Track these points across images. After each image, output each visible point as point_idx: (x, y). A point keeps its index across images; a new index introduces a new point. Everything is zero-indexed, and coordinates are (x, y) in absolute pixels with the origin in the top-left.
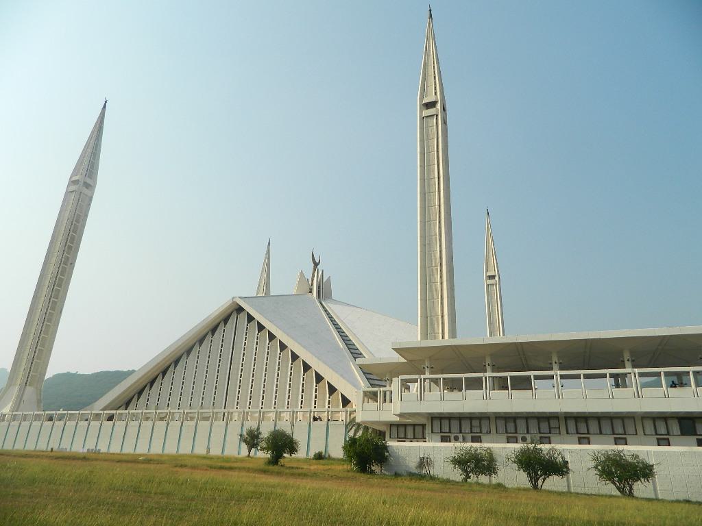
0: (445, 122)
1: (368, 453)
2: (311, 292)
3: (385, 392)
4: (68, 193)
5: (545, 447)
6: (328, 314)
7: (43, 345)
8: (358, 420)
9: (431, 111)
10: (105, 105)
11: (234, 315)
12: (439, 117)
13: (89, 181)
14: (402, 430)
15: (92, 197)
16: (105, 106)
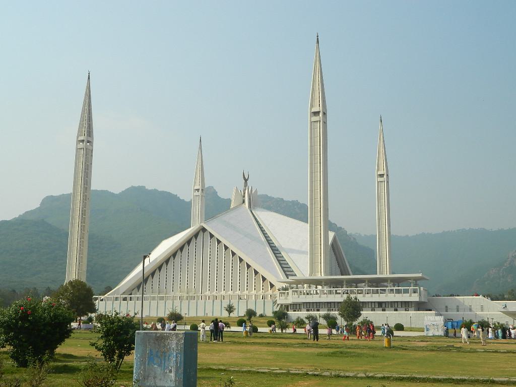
0: (325, 123)
1: (281, 317)
2: (244, 202)
3: (288, 293)
4: (78, 150)
5: (332, 313)
6: (257, 222)
7: (82, 254)
8: (278, 302)
9: (315, 118)
10: (89, 76)
11: (201, 233)
12: (321, 123)
13: (90, 139)
14: (295, 305)
15: (92, 150)
16: (89, 78)
